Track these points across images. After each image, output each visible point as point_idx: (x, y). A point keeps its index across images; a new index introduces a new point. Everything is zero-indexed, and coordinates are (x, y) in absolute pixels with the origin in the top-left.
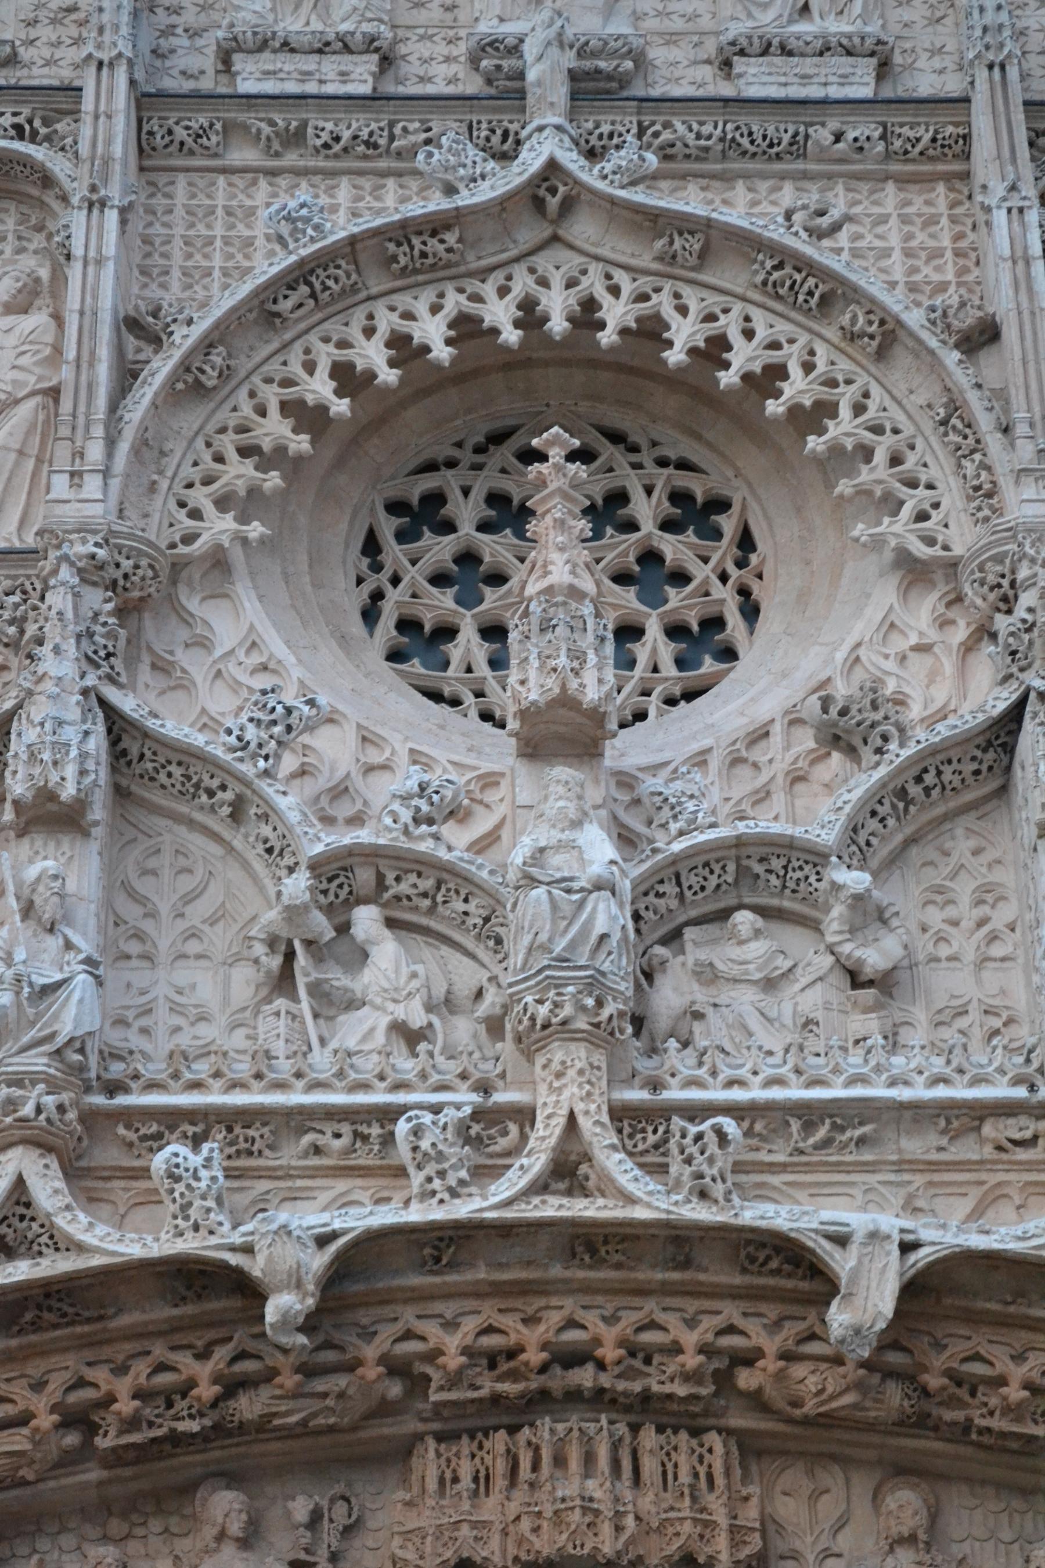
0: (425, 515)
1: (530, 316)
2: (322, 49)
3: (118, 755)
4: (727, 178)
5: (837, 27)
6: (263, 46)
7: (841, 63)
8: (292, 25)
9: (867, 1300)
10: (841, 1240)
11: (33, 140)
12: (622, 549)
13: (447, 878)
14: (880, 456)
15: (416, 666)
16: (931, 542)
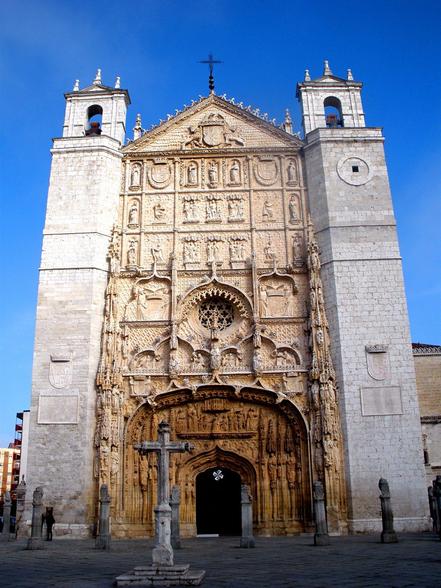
0: (204, 308)
1: (213, 293)
5: (241, 259)
9: (237, 391)
12: (222, 311)
13: (205, 352)
15: (204, 324)
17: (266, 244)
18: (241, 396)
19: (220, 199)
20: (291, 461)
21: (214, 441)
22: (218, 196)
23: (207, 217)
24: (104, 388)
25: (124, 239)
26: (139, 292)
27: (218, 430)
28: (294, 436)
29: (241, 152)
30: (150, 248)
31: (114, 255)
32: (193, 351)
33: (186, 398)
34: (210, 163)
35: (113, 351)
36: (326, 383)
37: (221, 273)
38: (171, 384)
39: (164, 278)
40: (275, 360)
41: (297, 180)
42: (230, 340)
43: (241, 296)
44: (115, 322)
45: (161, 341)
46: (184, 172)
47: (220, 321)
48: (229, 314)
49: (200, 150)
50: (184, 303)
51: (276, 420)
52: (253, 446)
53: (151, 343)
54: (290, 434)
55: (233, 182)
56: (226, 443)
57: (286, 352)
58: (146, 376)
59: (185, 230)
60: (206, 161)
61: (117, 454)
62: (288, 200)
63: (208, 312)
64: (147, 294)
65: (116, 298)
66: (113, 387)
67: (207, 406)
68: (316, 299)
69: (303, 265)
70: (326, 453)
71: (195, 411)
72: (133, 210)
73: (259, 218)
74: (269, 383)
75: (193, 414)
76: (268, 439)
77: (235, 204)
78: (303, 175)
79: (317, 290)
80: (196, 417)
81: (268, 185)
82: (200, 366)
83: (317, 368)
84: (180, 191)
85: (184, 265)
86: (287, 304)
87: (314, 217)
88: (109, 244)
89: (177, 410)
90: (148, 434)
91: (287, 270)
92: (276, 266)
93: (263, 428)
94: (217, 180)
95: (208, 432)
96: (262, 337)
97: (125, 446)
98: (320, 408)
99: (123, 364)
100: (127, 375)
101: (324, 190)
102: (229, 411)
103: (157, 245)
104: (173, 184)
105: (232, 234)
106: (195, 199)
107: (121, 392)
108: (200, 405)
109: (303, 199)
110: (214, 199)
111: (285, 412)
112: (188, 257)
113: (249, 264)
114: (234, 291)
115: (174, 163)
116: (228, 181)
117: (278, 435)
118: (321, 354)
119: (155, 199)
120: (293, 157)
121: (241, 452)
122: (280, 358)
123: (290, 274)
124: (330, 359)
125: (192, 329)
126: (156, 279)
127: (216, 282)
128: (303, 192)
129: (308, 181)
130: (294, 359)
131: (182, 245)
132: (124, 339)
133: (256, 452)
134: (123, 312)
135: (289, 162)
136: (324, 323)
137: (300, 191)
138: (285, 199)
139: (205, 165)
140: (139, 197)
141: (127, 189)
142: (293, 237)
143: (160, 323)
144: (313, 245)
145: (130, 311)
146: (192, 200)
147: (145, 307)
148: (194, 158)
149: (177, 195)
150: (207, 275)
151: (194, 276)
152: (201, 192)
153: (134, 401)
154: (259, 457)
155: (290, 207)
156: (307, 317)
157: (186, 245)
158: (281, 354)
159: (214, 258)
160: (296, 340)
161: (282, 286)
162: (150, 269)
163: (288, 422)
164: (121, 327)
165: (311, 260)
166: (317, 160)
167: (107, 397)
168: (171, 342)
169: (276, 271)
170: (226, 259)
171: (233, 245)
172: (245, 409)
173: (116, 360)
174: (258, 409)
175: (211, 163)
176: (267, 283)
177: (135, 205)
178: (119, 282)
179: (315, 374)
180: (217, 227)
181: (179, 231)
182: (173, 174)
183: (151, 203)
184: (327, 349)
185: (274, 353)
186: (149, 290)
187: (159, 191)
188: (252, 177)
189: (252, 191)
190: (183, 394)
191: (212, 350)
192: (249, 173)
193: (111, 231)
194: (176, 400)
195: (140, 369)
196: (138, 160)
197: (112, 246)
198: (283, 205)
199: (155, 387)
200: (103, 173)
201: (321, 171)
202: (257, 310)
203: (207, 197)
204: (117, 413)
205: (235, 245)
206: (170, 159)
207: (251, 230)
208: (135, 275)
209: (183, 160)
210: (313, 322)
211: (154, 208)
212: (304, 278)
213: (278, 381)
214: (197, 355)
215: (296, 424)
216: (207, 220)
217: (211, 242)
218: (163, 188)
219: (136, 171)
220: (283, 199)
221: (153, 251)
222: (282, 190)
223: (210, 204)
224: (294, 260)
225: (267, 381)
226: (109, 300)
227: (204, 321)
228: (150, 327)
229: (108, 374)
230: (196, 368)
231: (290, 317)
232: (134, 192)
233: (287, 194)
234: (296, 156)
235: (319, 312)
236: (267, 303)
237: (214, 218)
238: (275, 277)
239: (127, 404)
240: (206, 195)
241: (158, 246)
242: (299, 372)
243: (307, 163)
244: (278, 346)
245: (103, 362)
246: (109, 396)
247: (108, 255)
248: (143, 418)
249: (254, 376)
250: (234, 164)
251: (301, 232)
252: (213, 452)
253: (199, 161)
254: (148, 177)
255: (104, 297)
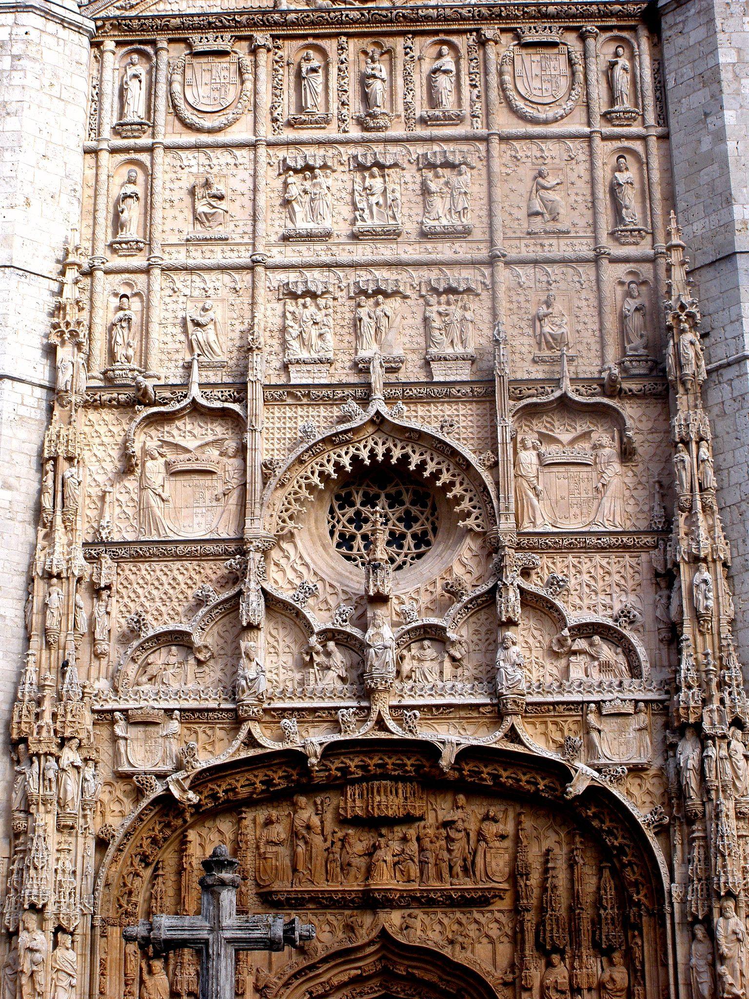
1: (373, 455)
2: (315, 363)
3: (266, 600)
4: (428, 403)
5: (459, 350)
6: (298, 362)
7: (460, 363)
8: (304, 355)
9: (448, 758)
10: (443, 743)
11: (234, 402)
12: (400, 510)
13: (350, 635)
14: (467, 499)
15: (344, 550)
16: (478, 526)
17: (539, 303)
18: (457, 774)
19: (395, 165)
20: (613, 980)
21: (375, 914)
22: (393, 154)
23: (355, 219)
24: (33, 749)
25: (98, 288)
26: (146, 453)
27: (386, 880)
28: (623, 900)
29: (464, 19)
30: (181, 314)
31: (67, 336)
32: (312, 633)
33: (287, 778)
34: (365, 53)
35: (63, 635)
36: (724, 737)
37: (399, 392)
38: (242, 735)
39: (224, 409)
40: (563, 662)
41: (636, 105)
42: (425, 599)
43: (458, 465)
44: (70, 544)
45: (212, 603)
46: (286, 79)
47: (395, 540)
48: (422, 518)
49: (334, 11)
50: (283, 485)
51: (565, 849)
52: (494, 932)
53: (180, 609)
54: (610, 894)
55: (438, 113)
56: (410, 921)
57: (597, 638)
58: (166, 710)
59: (286, 261)
60: (353, 45)
61: (71, 955)
62: (608, 168)
63: (358, 513)
64: (171, 457)
65: (74, 470)
66: (61, 746)
67: (355, 803)
68: (692, 476)
69: (651, 370)
70: (723, 959)
71: (316, 821)
72: (126, 197)
73: (515, 225)
74: (545, 734)
75: (308, 828)
76: (541, 910)
77: (442, 180)
78: (656, 89)
79: (694, 446)
80: (317, 840)
81: (546, 122)
82: (330, 680)
83: (695, 690)
84: (271, 138)
85: (285, 367)
86: (600, 490)
87: (689, 223)
88: (51, 302)
89: (261, 815)
90: (171, 892)
91: (602, 386)
92: (568, 371)
93: (527, 874)
94: (388, 105)
95: (354, 885)
96: (522, 591)
97: (98, 931)
98: (704, 815)
99: (94, 673)
100: (107, 707)
101: (720, 136)
102: (421, 818)
103: (201, 305)
104: (250, 117)
105: (433, 274)
106: (319, 163)
107: (86, 760)
108: (331, 802)
109: (655, 163)
110: (377, 164)
111: (595, 823)
112: (295, 344)
113: (484, 365)
114: (436, 449)
115: (254, 52)
116: (420, 109)
117: (574, 896)
118: (707, 645)
119: (193, 162)
120: (625, 34)
121: (458, 947)
122: (580, 658)
123: (611, 396)
124: (734, 663)
125: (306, 565)
126: (196, 410)
127: (383, 420)
128: (653, 142)
129: (671, 108)
130: (621, 659)
131: (279, 307)
132: (99, 597)
133: (504, 949)
134: (92, 514)
135: (611, 48)
136: (714, 550)
137: (644, 138)
138: (599, 163)
139: (351, 58)
140: (144, 157)
141: (106, 132)
142: (621, 283)
143: (211, 548)
144: (683, 307)
145: (118, 510)
146: (309, 168)
147: (164, 496)
148: (316, 36)
149: (262, 150)
150: (355, 399)
151: (316, 402)
152: (341, 143)
153: (128, 788)
154: (512, 966)
155: (614, 189)
156: (663, 531)
157: (291, 306)
158: (581, 644)
159: (375, 347)
160: (630, 600)
161: (586, 435)
162: (178, 381)
163: (605, 857)
164: (90, 558)
165: (677, 355)
166: (699, 43)
167: (42, 775)
168: (243, 606)
169: (568, 387)
170: (413, 351)
171: (435, 308)
172: (469, 814)
173: (72, 662)
174: (511, 815)
175: (369, 50)
176: (539, 425)
177: (131, 181)
178: (84, 420)
179: (688, 708)
180: (386, 252)
181: (270, 261)
182: (249, 85)
183: (183, 174)
184: (725, 630)
185: (561, 642)
186: (176, 446)
187: (205, 138)
188: (494, 94)
189: (495, 140)
190: (280, 766)
191: (371, 631)
192: (486, 81)
193: (58, 261)
194: (258, 785)
195: (146, 687)
196: (141, 42)
197: (60, 308)
198: (592, 182)
199: (193, 743)
200: (30, 81)
201: (711, 78)
202: (507, 508)
203: (355, 157)
204: (72, 828)
205: (442, 309)
206: (240, 38)
207: (492, 261)
208: (132, 399)
209: (280, 42)
210: (683, 546)
211: (192, 192)
212: (654, 410)
213: (574, 727)
214: (324, 646)
215: (630, 864)
216: (355, 229)
217: (368, 296)
218: (219, 130)
219: (135, 76)
220: (592, 164)
221: (190, 324)
222: (589, 138)
223: (364, 178)
224: (624, 354)
225: (540, 728)
226: (51, 474)
227: (346, 541)
228: (178, 557)
229: (47, 706)
230: (320, 686)
231: (612, 529)
232: (131, 142)
233: (603, 149)
234: (633, 29)
235: (701, 516)
236: (540, 488)
237: (377, 222)
238: (565, 406)
239: (105, 798)
240: (352, 150)
241: (205, 310)
242: (637, 702)
243: (669, 51)
244: (574, 618)
245: (31, 667)
246: (51, 774)
247: (47, 336)
248: (154, 841)
249: (497, 713)
250: (440, 55)
251: (646, 270)
252: (372, 949)
253: (330, 45)
254: (171, 94)
255: (34, 465)
